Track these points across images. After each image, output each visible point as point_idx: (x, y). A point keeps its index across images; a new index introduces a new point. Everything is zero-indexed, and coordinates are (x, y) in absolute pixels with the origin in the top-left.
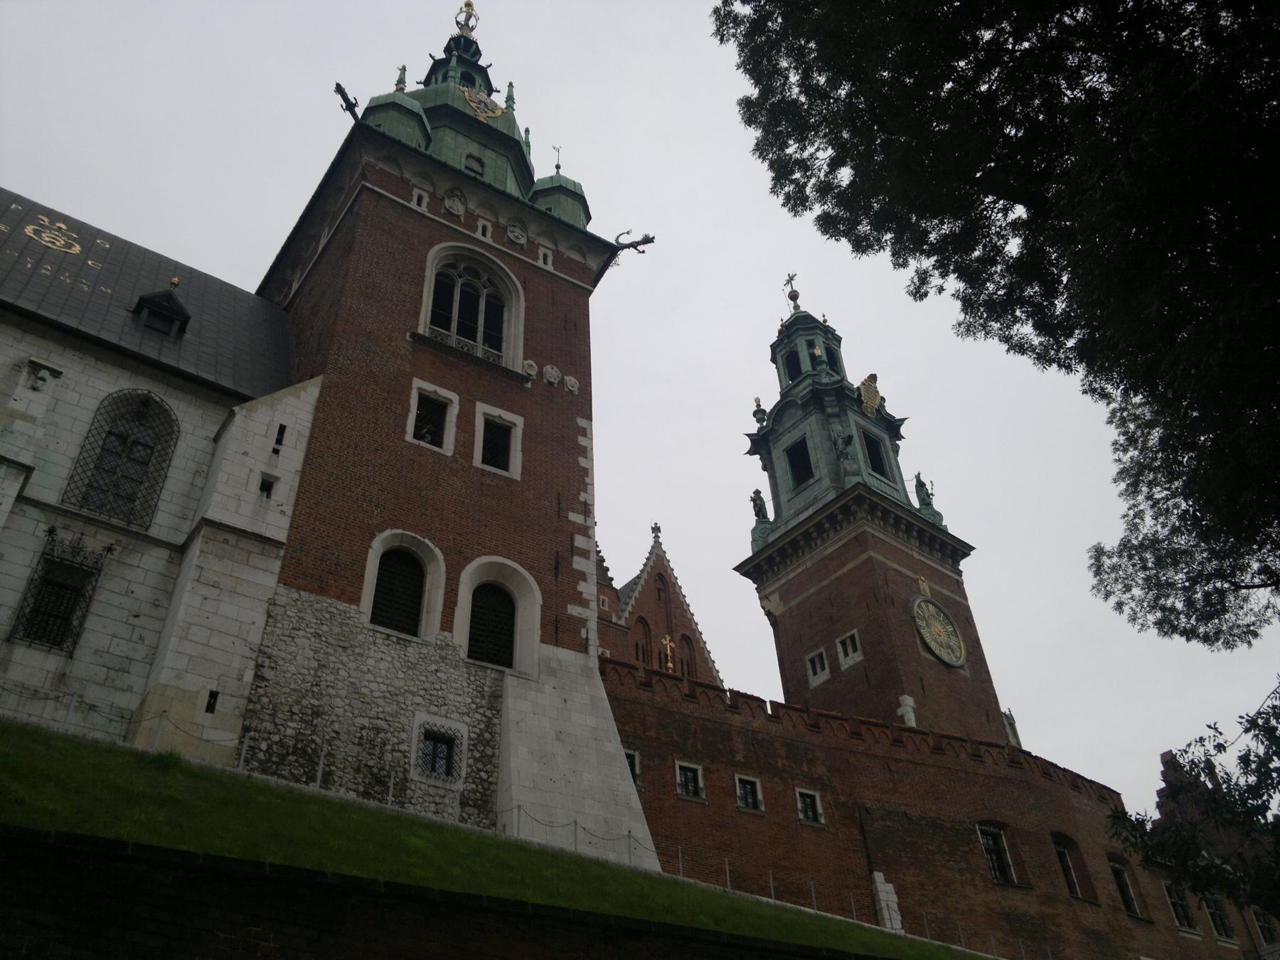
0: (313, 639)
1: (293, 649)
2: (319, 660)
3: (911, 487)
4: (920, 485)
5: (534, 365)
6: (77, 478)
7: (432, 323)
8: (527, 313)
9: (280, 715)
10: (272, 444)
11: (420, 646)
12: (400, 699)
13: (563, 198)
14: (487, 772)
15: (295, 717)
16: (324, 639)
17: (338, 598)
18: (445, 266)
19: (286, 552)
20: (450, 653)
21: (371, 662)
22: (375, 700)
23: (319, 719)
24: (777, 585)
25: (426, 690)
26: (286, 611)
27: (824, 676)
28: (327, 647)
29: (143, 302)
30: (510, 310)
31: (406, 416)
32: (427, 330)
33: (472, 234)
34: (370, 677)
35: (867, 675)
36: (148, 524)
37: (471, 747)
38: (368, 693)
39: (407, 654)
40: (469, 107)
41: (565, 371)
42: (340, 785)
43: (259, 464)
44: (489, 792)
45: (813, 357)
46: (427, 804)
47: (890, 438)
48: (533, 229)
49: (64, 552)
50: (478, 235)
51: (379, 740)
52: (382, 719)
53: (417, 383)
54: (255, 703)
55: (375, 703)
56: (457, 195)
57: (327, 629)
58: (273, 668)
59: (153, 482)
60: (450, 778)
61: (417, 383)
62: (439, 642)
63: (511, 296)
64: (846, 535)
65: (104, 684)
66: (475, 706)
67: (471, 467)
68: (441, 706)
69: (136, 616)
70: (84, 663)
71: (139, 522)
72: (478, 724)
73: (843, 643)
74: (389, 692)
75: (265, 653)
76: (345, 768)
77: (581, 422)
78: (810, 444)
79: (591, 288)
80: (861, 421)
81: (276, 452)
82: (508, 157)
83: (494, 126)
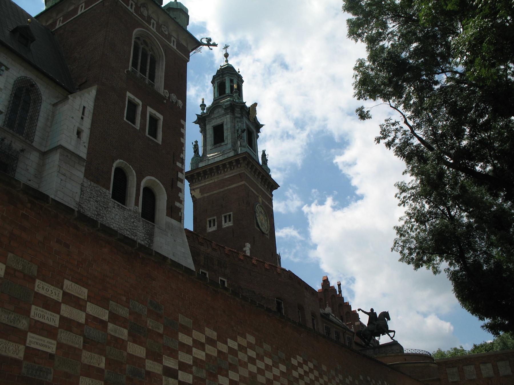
1: (89, 206)
3: (260, 155)
4: (264, 155)
8: (165, 68)
17: (103, 187)
24: (199, 186)
25: (130, 229)
27: (213, 229)
34: (113, 221)
35: (233, 232)
45: (232, 87)
47: (256, 131)
64: (236, 172)
73: (225, 217)
74: (119, 228)
78: (225, 127)
80: (247, 122)
81: (82, 118)
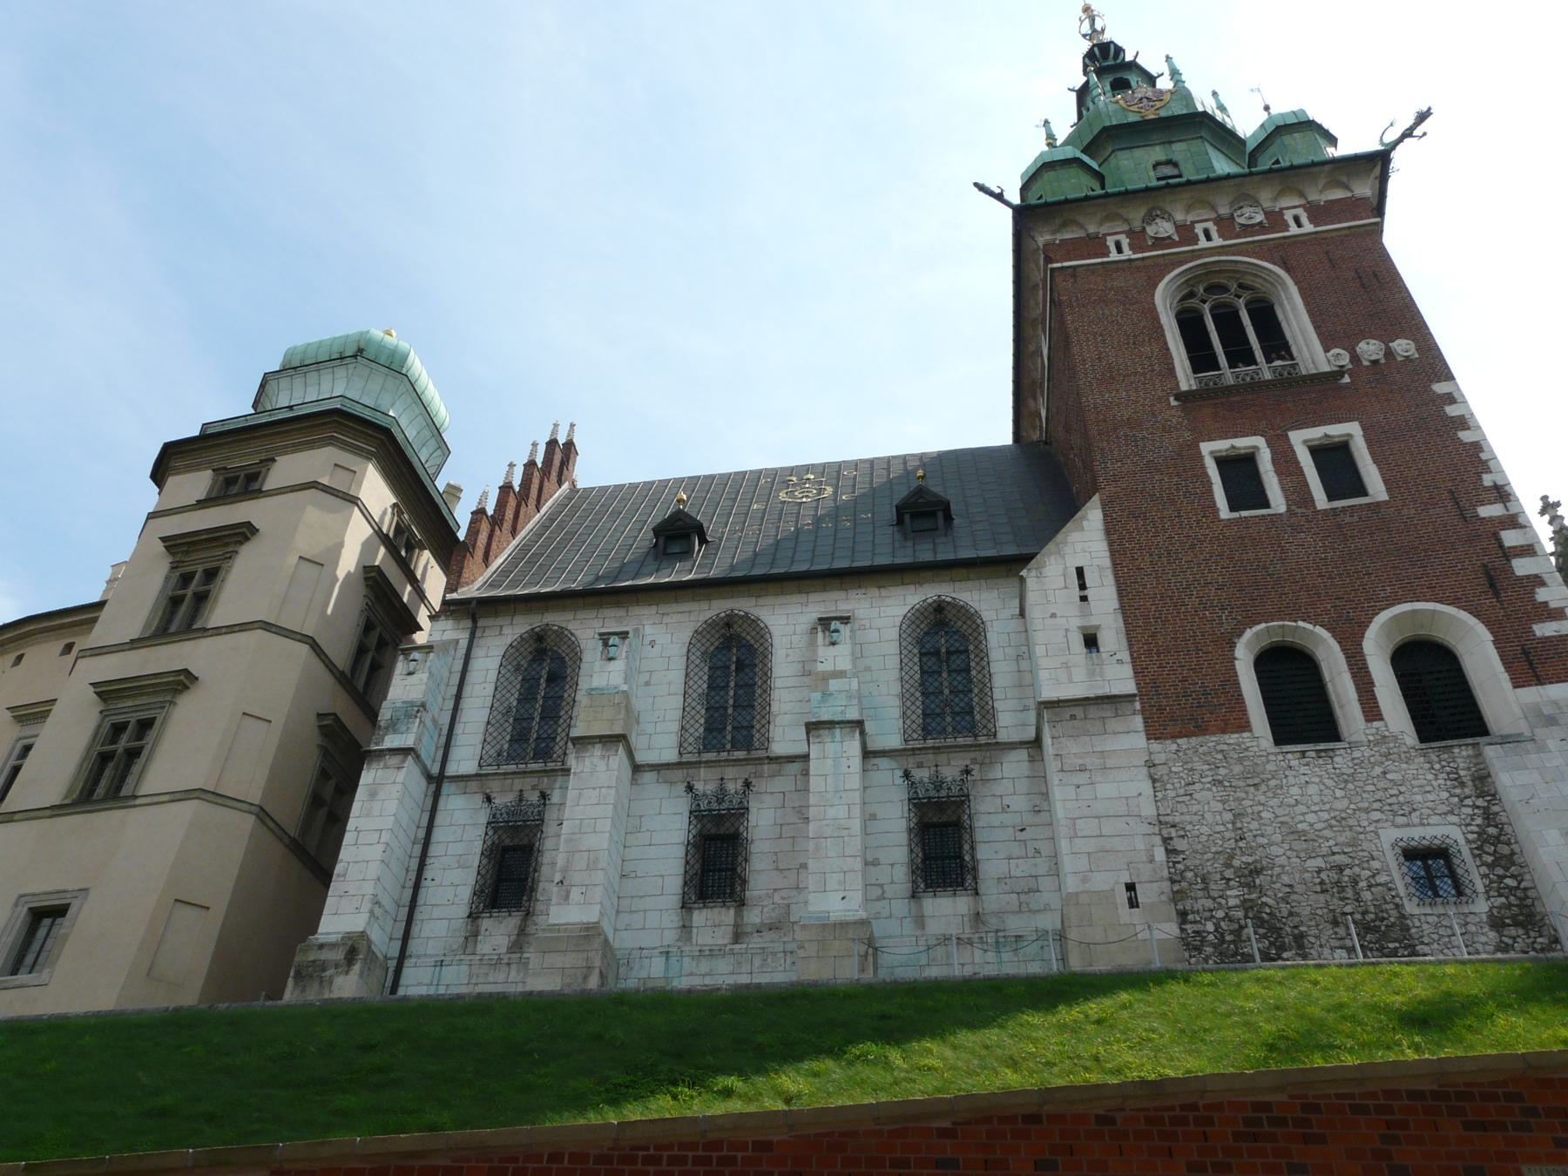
0: (1214, 789)
1: (1195, 808)
2: (1231, 810)
5: (1342, 352)
6: (909, 712)
7: (1195, 371)
8: (1304, 297)
9: (1212, 886)
10: (1076, 592)
11: (1349, 751)
12: (1351, 822)
13: (1287, 139)
14: (1513, 876)
15: (1232, 883)
16: (1227, 784)
17: (1224, 731)
18: (1183, 299)
19: (1141, 703)
20: (1392, 745)
21: (1295, 791)
22: (1321, 834)
23: (1262, 877)
25: (1380, 801)
26: (1170, 768)
28: (1235, 792)
29: (901, 510)
30: (1281, 305)
31: (1210, 491)
32: (1192, 382)
33: (1196, 247)
36: (993, 730)
37: (1476, 852)
38: (1308, 828)
39: (1336, 766)
40: (1131, 114)
41: (1387, 337)
42: (1321, 946)
43: (1072, 621)
44: (1529, 902)
46: (1447, 939)
48: (1266, 197)
49: (927, 790)
50: (1203, 243)
51: (1346, 879)
52: (1338, 853)
53: (1206, 448)
54: (1180, 882)
55: (1321, 837)
56: (1157, 216)
57: (1227, 771)
58: (1183, 837)
59: (981, 686)
60: (1464, 899)
61: (1206, 448)
62: (1371, 738)
63: (1275, 287)
65: (1020, 911)
66: (1456, 799)
67: (1317, 512)
68: (1410, 813)
69: (1022, 830)
70: (993, 897)
71: (985, 732)
72: (1473, 820)
74: (1334, 818)
75: (1167, 823)
76: (1317, 925)
77: (1440, 388)
79: (1378, 220)
81: (1084, 599)
82: (1201, 137)
83: (1170, 113)
